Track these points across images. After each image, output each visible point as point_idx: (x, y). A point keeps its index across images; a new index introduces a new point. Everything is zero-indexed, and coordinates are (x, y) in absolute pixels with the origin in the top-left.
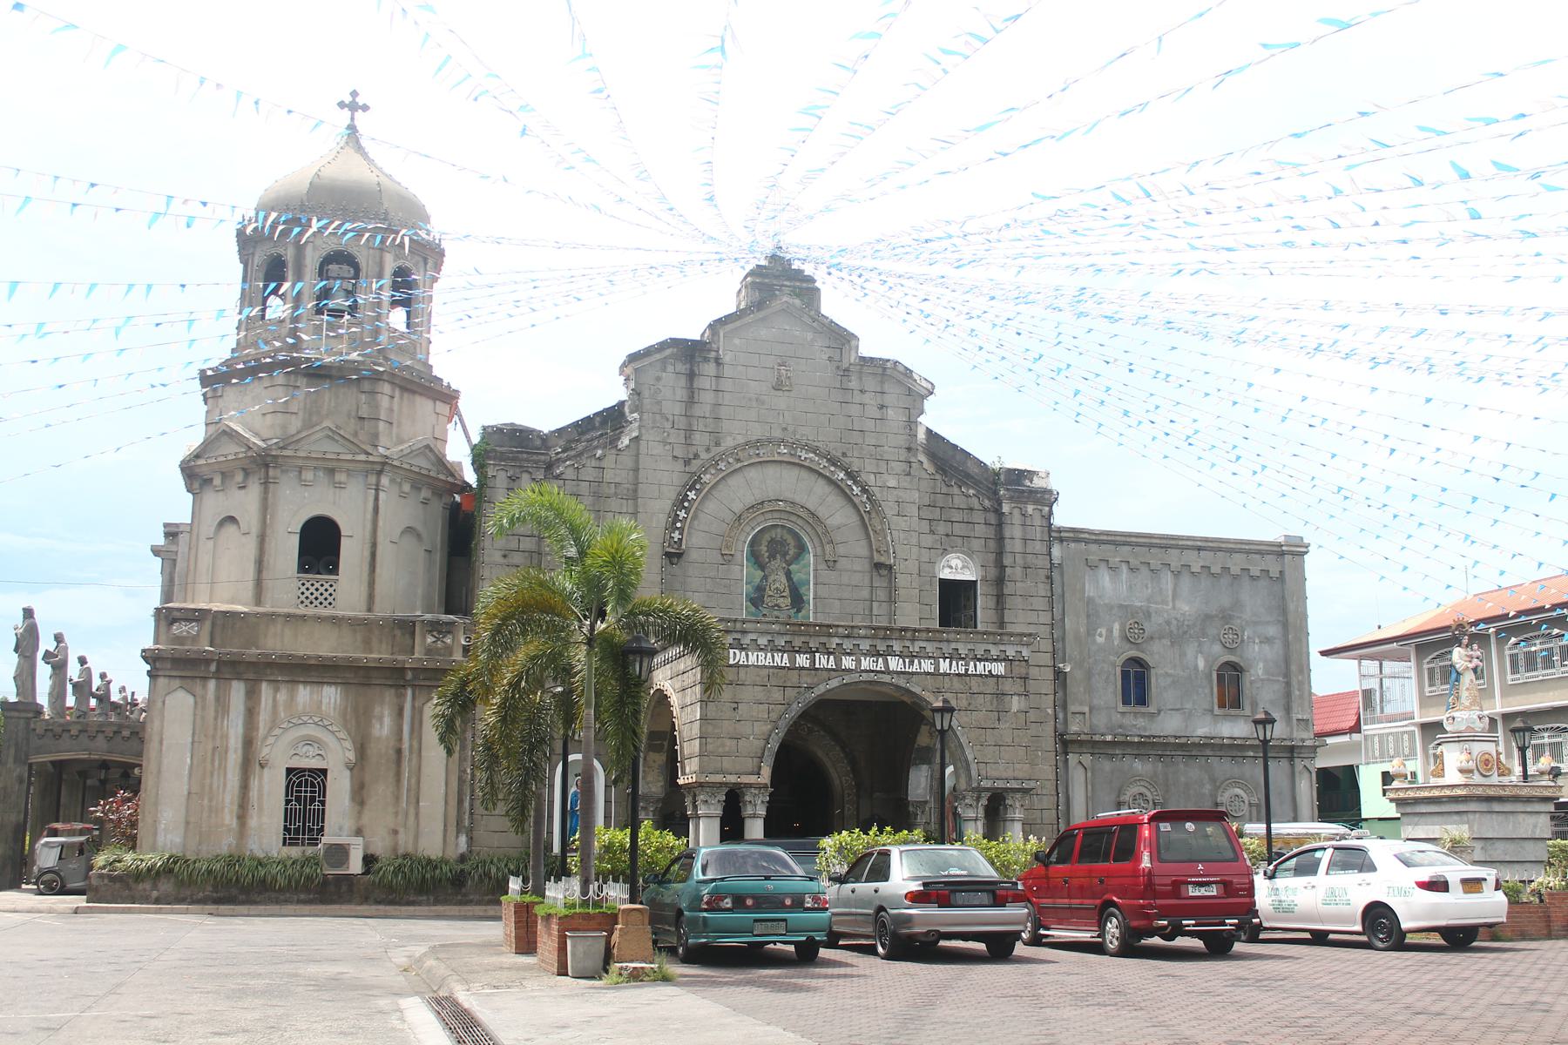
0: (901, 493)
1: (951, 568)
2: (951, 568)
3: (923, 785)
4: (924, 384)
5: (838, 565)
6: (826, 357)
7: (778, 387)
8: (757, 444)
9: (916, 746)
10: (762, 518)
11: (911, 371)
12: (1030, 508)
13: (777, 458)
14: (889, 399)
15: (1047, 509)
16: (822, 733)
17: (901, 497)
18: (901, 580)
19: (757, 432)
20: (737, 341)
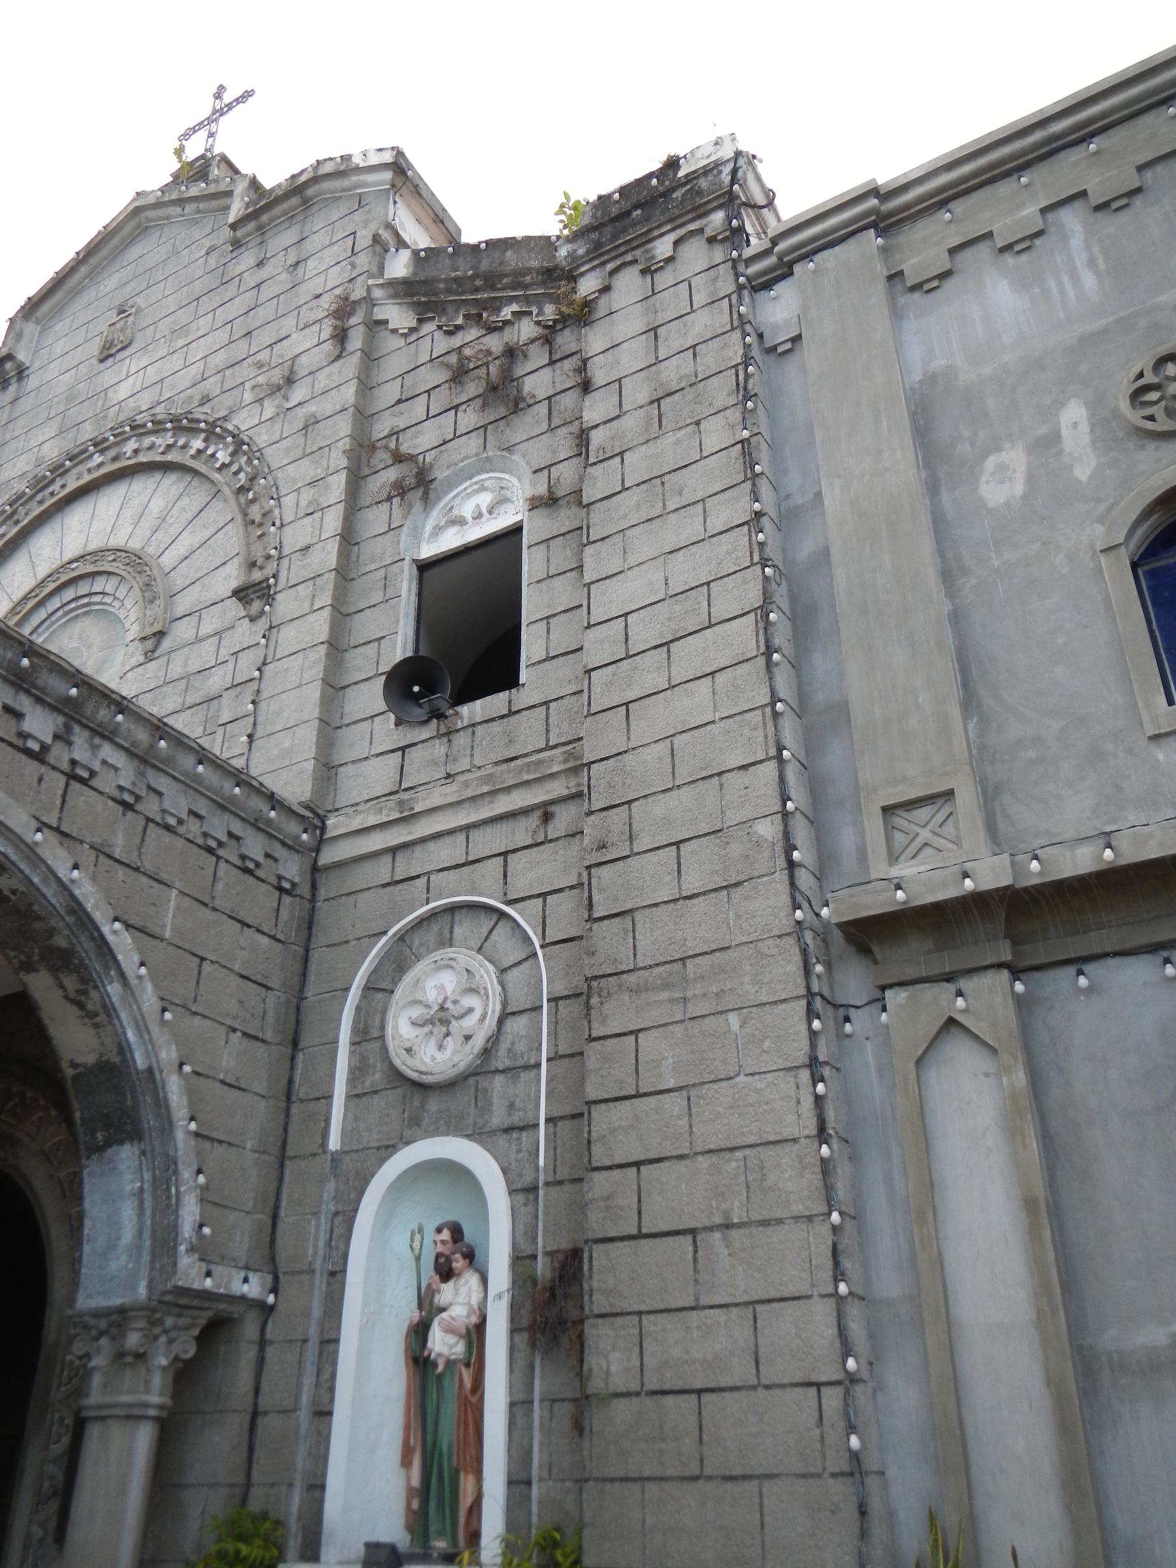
0: (312, 408)
1: (461, 522)
2: (461, 522)
3: (128, 1235)
4: (374, 160)
5: (166, 644)
6: (203, 252)
7: (108, 353)
8: (59, 470)
9: (70, 1072)
10: (42, 614)
11: (346, 158)
12: (663, 247)
13: (87, 478)
14: (315, 242)
15: (718, 217)
16: (54, 1113)
17: (314, 415)
18: (286, 604)
19: (52, 452)
20: (58, 327)
